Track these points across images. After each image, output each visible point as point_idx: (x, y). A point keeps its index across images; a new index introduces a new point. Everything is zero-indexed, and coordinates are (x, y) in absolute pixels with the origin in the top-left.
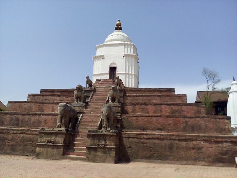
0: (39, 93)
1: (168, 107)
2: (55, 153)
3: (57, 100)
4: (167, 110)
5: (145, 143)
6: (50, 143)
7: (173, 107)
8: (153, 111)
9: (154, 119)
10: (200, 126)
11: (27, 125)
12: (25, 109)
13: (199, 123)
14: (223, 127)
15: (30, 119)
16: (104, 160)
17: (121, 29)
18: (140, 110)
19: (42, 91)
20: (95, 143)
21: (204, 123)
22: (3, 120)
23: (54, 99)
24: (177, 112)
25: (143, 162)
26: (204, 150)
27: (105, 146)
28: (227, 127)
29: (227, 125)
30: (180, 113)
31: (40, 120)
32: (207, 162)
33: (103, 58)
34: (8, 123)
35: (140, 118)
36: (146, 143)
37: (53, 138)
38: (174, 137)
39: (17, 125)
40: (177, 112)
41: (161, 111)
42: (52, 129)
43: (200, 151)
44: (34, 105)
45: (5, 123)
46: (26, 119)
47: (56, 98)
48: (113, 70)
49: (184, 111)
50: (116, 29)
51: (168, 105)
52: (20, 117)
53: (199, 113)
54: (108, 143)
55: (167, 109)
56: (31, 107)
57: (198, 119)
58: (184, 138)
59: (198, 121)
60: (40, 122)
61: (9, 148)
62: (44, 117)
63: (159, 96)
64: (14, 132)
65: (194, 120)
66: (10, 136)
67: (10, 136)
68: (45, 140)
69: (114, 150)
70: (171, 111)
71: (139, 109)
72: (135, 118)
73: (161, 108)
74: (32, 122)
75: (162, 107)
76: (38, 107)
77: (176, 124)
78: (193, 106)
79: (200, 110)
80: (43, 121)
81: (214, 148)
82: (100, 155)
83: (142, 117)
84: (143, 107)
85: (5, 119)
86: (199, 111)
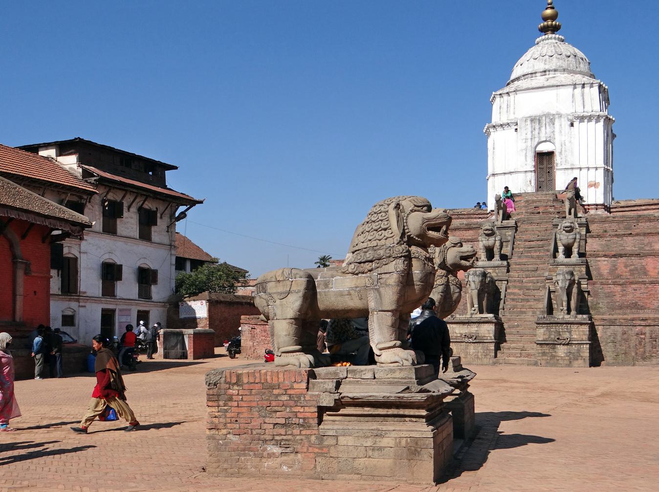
2: (480, 354)
5: (641, 334)
6: (470, 339)
16: (570, 362)
17: (555, 29)
18: (628, 269)
20: (553, 336)
27: (570, 341)
35: (630, 289)
36: (644, 334)
37: (473, 329)
48: (544, 160)
50: (544, 30)
68: (459, 335)
69: (588, 346)
71: (626, 266)
72: (619, 288)
82: (563, 356)
83: (634, 286)
84: (635, 260)
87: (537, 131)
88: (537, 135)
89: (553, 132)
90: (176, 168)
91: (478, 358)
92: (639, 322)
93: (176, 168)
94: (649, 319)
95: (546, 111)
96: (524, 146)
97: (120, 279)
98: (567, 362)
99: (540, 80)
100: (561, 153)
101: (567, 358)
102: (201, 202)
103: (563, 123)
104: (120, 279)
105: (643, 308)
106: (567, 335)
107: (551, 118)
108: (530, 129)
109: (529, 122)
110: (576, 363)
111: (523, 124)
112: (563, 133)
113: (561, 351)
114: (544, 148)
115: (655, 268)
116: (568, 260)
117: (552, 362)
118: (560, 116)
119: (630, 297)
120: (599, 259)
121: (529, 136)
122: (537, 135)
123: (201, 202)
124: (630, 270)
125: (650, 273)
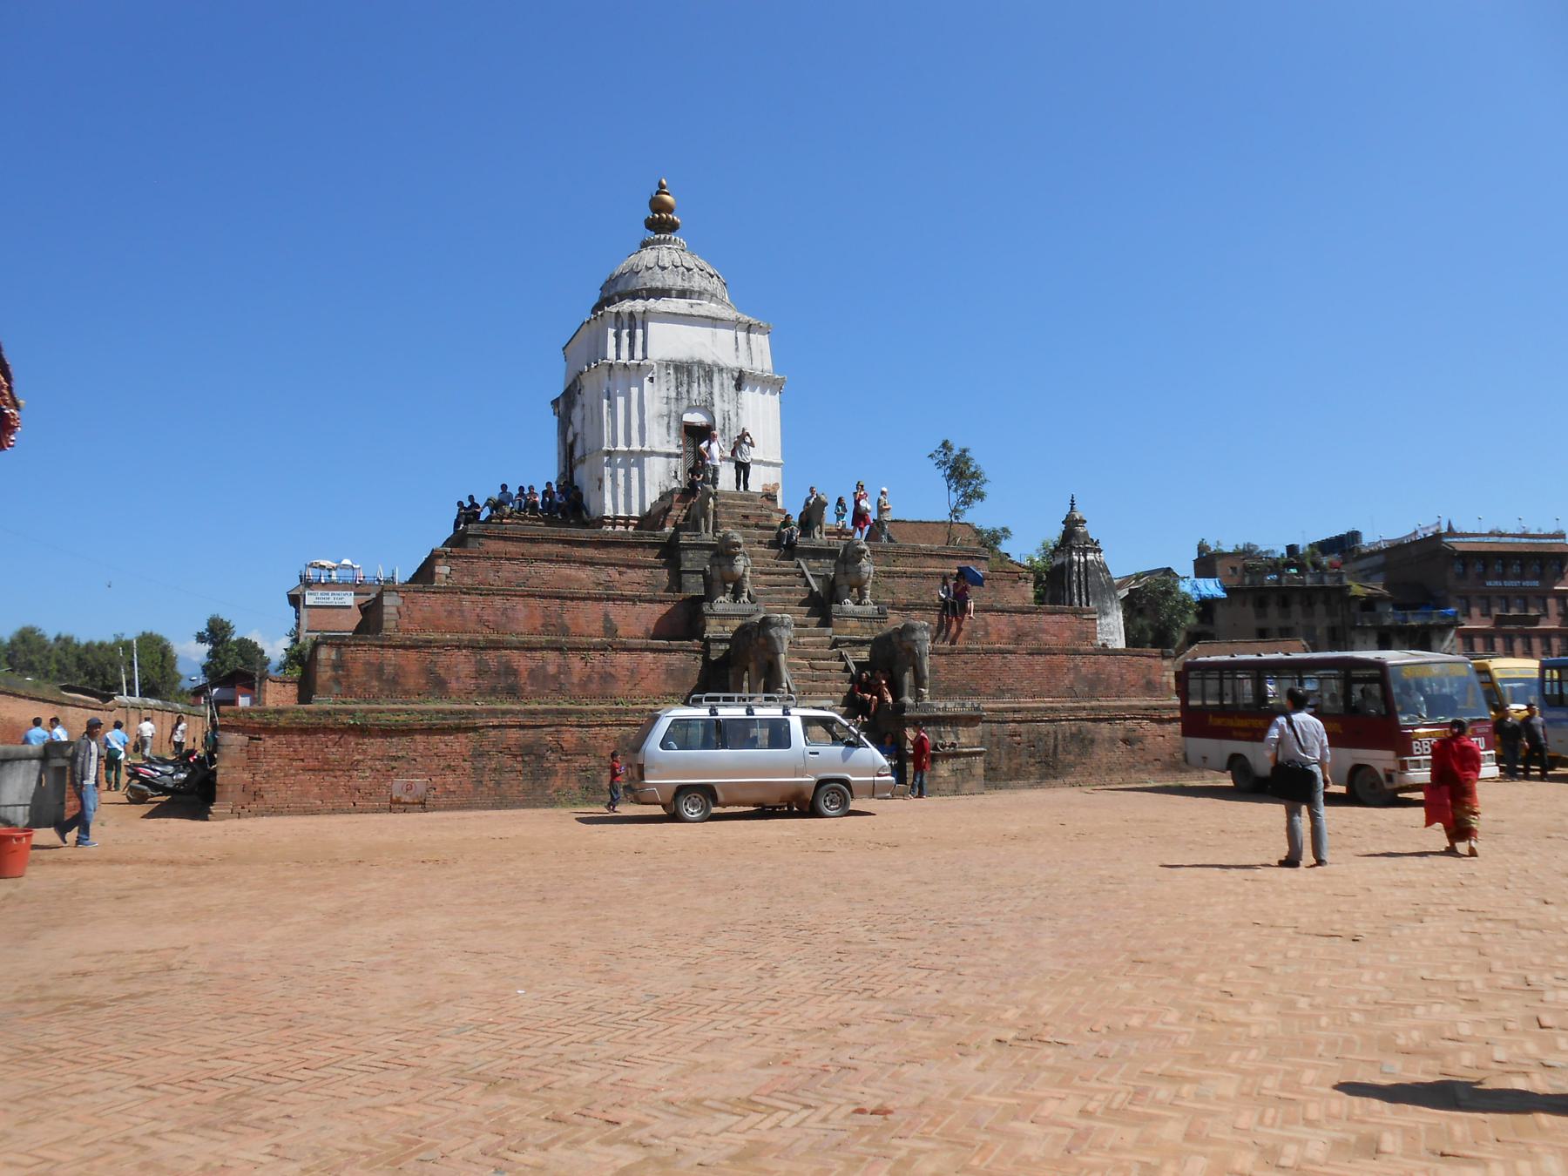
1: (1005, 618)
3: (578, 580)
7: (1017, 618)
9: (997, 659)
11: (560, 690)
12: (480, 620)
14: (1156, 678)
15: (565, 670)
17: (673, 227)
22: (442, 671)
23: (568, 579)
24: (1027, 634)
25: (1014, 788)
26: (1150, 740)
31: (612, 670)
32: (1150, 773)
33: (651, 380)
34: (470, 684)
35: (958, 660)
38: (1083, 714)
39: (513, 692)
40: (1027, 634)
41: (987, 634)
43: (1140, 745)
44: (520, 607)
45: (454, 685)
46: (552, 669)
47: (573, 572)
49: (1045, 631)
51: (1003, 611)
53: (1080, 638)
56: (510, 613)
58: (1106, 714)
60: (607, 678)
61: (574, 778)
62: (623, 659)
64: (584, 721)
66: (567, 736)
67: (570, 737)
74: (575, 680)
76: (538, 612)
77: (1052, 669)
85: (448, 668)
87: (685, 388)
88: (685, 395)
92: (1010, 716)
95: (697, 357)
96: (665, 410)
97: (1354, 536)
98: (952, 787)
99: (680, 305)
100: (723, 431)
103: (726, 382)
104: (1354, 536)
105: (976, 693)
106: (950, 739)
107: (710, 372)
108: (673, 382)
110: (967, 786)
111: (663, 372)
113: (943, 769)
114: (698, 419)
116: (858, 609)
118: (721, 370)
121: (673, 394)
122: (685, 395)
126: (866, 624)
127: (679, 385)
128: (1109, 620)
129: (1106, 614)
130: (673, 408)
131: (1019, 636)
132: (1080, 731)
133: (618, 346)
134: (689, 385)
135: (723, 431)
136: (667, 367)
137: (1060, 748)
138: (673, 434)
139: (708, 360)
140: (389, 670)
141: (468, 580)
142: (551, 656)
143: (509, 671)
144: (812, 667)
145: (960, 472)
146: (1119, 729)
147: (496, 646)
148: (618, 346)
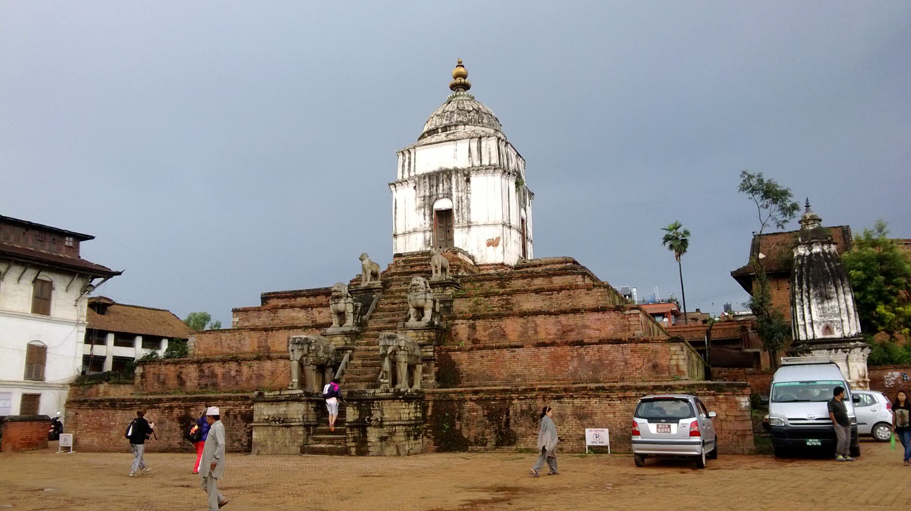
0: (258, 303)
1: (552, 319)
4: (547, 328)
7: (562, 318)
8: (516, 334)
9: (507, 353)
10: (612, 363)
13: (610, 358)
14: (663, 362)
19: (266, 298)
21: (620, 356)
23: (293, 318)
28: (673, 362)
29: (675, 357)
30: (579, 333)
31: (262, 372)
37: (281, 409)
40: (572, 330)
41: (536, 332)
42: (277, 393)
45: (188, 384)
46: (233, 373)
49: (586, 327)
51: (550, 314)
52: (219, 369)
53: (623, 331)
54: (387, 416)
55: (549, 327)
57: (607, 347)
59: (606, 352)
60: (260, 377)
63: (538, 291)
65: (598, 351)
70: (558, 330)
71: (485, 330)
73: (536, 324)
75: (540, 319)
76: (255, 340)
77: (556, 360)
78: (613, 314)
79: (627, 323)
80: (266, 373)
81: (617, 414)
86: (626, 326)
88: (435, 192)
89: (450, 188)
90: (92, 238)
91: (285, 446)
93: (92, 238)
94: (482, 391)
98: (378, 449)
101: (379, 444)
102: (119, 274)
103: (460, 179)
109: (427, 180)
112: (460, 189)
114: (442, 204)
115: (514, 331)
117: (362, 449)
118: (457, 171)
119: (477, 366)
120: (456, 322)
122: (435, 192)
123: (119, 274)
124: (489, 334)
125: (509, 337)
126: (420, 334)
127: (431, 186)
128: (834, 303)
129: (829, 298)
130: (427, 201)
131: (565, 331)
132: (530, 409)
133: (403, 171)
134: (437, 186)
135: (458, 210)
136: (424, 178)
137: (512, 421)
138: (427, 218)
139: (451, 167)
140: (162, 377)
141: (246, 324)
142: (233, 366)
143: (214, 375)
144: (363, 366)
145: (772, 194)
146: (568, 406)
147: (208, 361)
148: (403, 171)
